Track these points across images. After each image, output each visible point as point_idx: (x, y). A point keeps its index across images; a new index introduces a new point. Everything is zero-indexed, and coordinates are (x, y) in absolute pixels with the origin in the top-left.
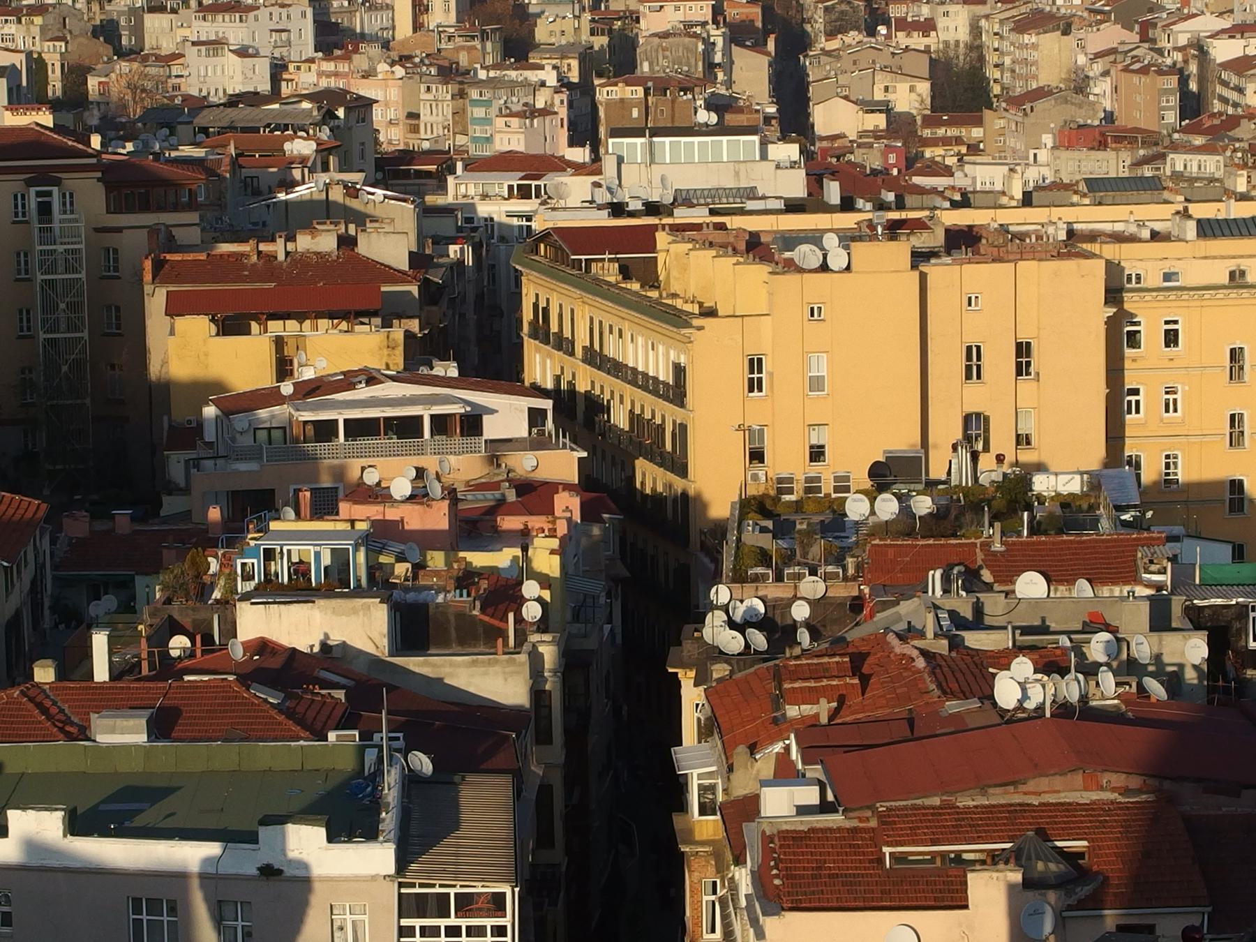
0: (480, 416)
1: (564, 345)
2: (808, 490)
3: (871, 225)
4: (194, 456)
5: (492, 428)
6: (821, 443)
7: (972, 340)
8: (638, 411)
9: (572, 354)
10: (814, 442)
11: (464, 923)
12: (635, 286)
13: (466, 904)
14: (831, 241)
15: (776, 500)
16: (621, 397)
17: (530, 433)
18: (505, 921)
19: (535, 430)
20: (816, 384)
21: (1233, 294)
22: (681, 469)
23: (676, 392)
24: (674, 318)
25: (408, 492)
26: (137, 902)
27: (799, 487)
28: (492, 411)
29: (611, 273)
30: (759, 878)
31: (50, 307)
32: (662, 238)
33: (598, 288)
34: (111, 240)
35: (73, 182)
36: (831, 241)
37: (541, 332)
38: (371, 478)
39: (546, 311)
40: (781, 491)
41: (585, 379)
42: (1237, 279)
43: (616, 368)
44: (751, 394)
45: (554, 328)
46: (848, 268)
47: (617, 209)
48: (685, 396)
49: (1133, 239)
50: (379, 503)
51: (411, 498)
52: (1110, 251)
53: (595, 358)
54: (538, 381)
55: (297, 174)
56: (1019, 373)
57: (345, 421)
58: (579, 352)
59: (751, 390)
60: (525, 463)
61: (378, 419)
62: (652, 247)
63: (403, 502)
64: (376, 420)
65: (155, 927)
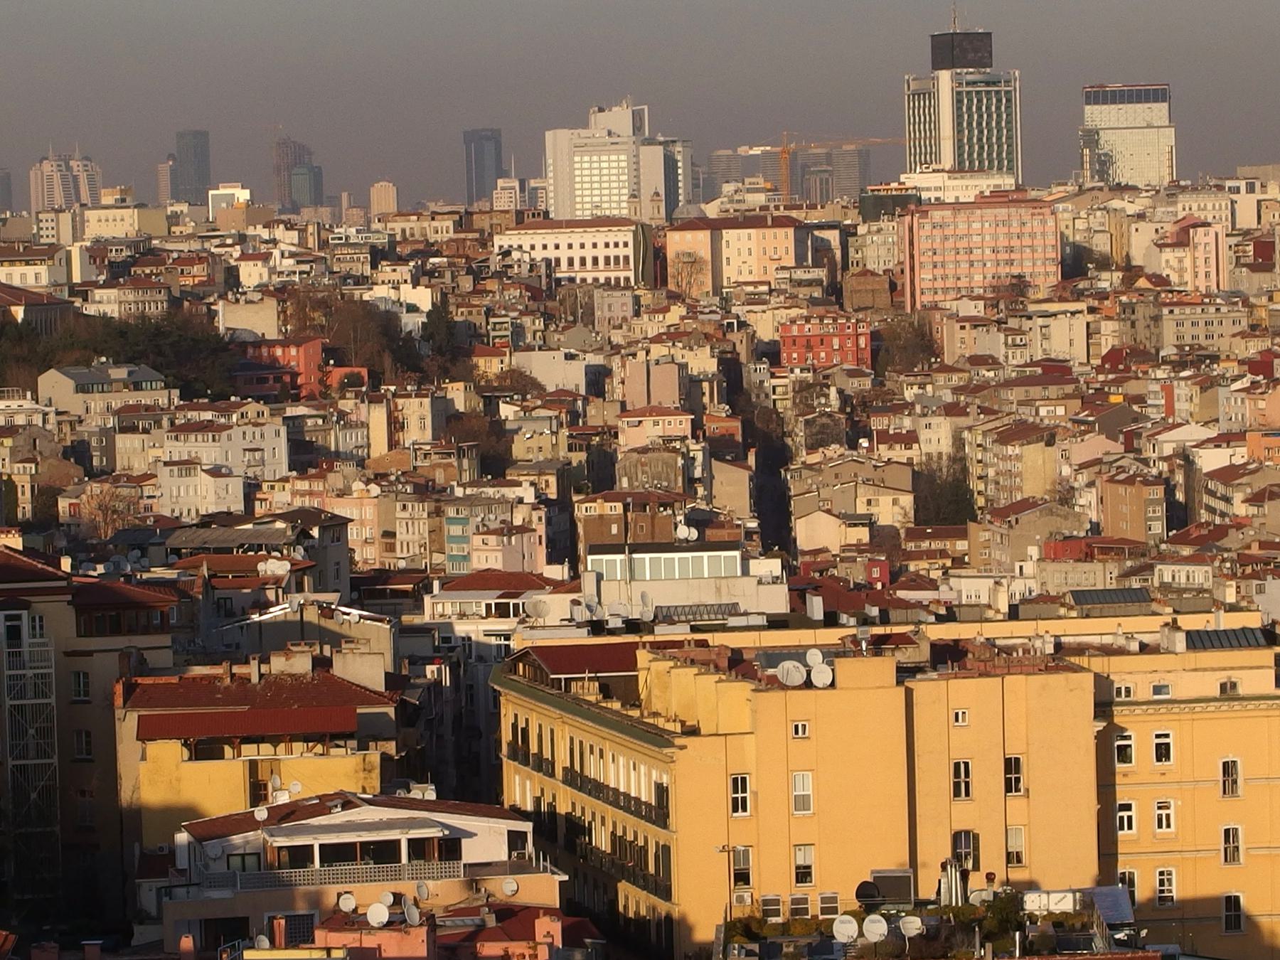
0: (459, 841)
1: (543, 766)
2: (794, 912)
3: (855, 641)
4: (167, 884)
5: (471, 852)
6: (808, 863)
7: (959, 756)
8: (619, 833)
9: (552, 775)
10: (800, 862)
12: (616, 705)
14: (815, 657)
15: (762, 922)
16: (603, 818)
17: (510, 857)
19: (515, 854)
20: (802, 803)
21: (1225, 706)
22: (666, 893)
23: (659, 812)
25: (385, 919)
27: (785, 909)
28: (471, 835)
29: (589, 691)
32: (643, 656)
33: (578, 708)
34: (81, 663)
36: (815, 657)
37: (520, 753)
38: (347, 904)
39: (525, 731)
40: (767, 913)
41: (566, 801)
42: (1228, 691)
43: (597, 789)
44: (735, 814)
45: (534, 748)
46: (832, 685)
47: (597, 627)
48: (668, 817)
49: (1121, 652)
50: (356, 930)
51: (389, 925)
53: (576, 779)
54: (518, 803)
55: (271, 595)
56: (1008, 789)
57: (321, 846)
58: (559, 772)
59: (735, 810)
60: (505, 887)
61: (354, 844)
62: (633, 665)
63: (380, 929)
64: (352, 845)
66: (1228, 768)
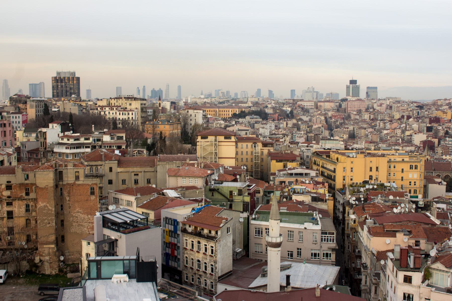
3: (358, 152)
7: (371, 166)
9: (319, 166)
11: (329, 236)
12: (328, 158)
13: (330, 233)
18: (334, 236)
23: (334, 171)
24: (334, 163)
26: (288, 231)
27: (355, 184)
29: (325, 157)
30: (369, 231)
31: (255, 158)
32: (331, 153)
34: (262, 150)
35: (258, 143)
36: (354, 154)
39: (316, 161)
42: (403, 160)
43: (325, 168)
45: (317, 163)
46: (356, 157)
47: (324, 149)
49: (389, 155)
52: (388, 156)
53: (323, 167)
58: (320, 166)
62: (330, 153)
65: (291, 234)
66: (403, 170)
